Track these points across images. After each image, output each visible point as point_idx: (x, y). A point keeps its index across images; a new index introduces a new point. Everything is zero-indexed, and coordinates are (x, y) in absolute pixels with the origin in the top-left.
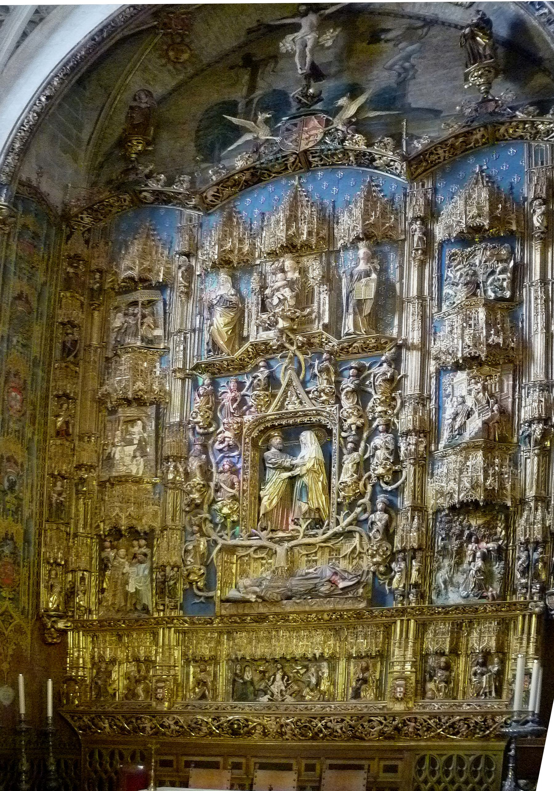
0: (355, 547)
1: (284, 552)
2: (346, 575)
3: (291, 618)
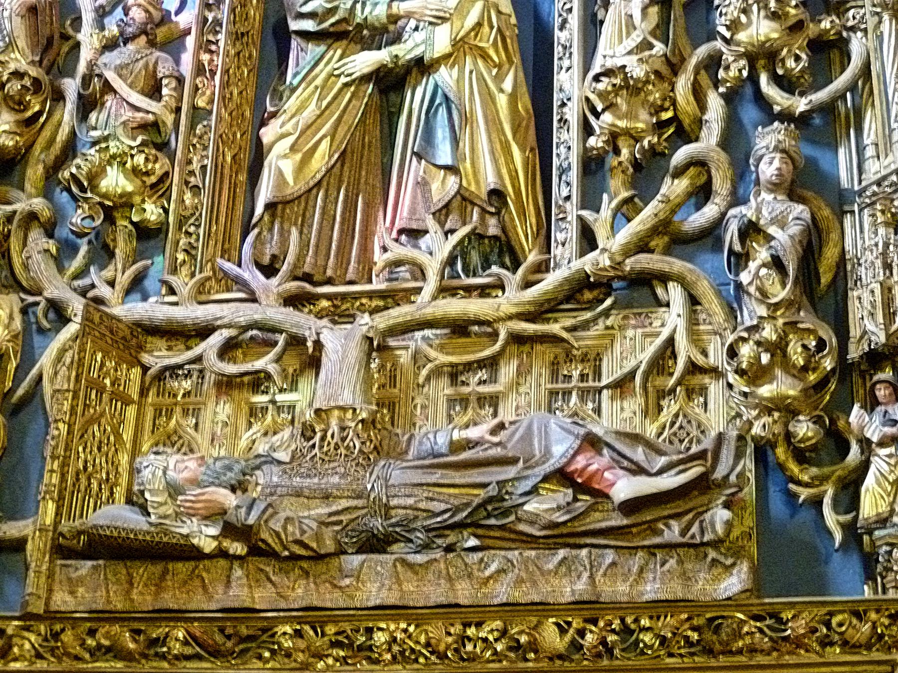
0: (670, 342)
1: (355, 352)
2: (639, 454)
3: (380, 638)
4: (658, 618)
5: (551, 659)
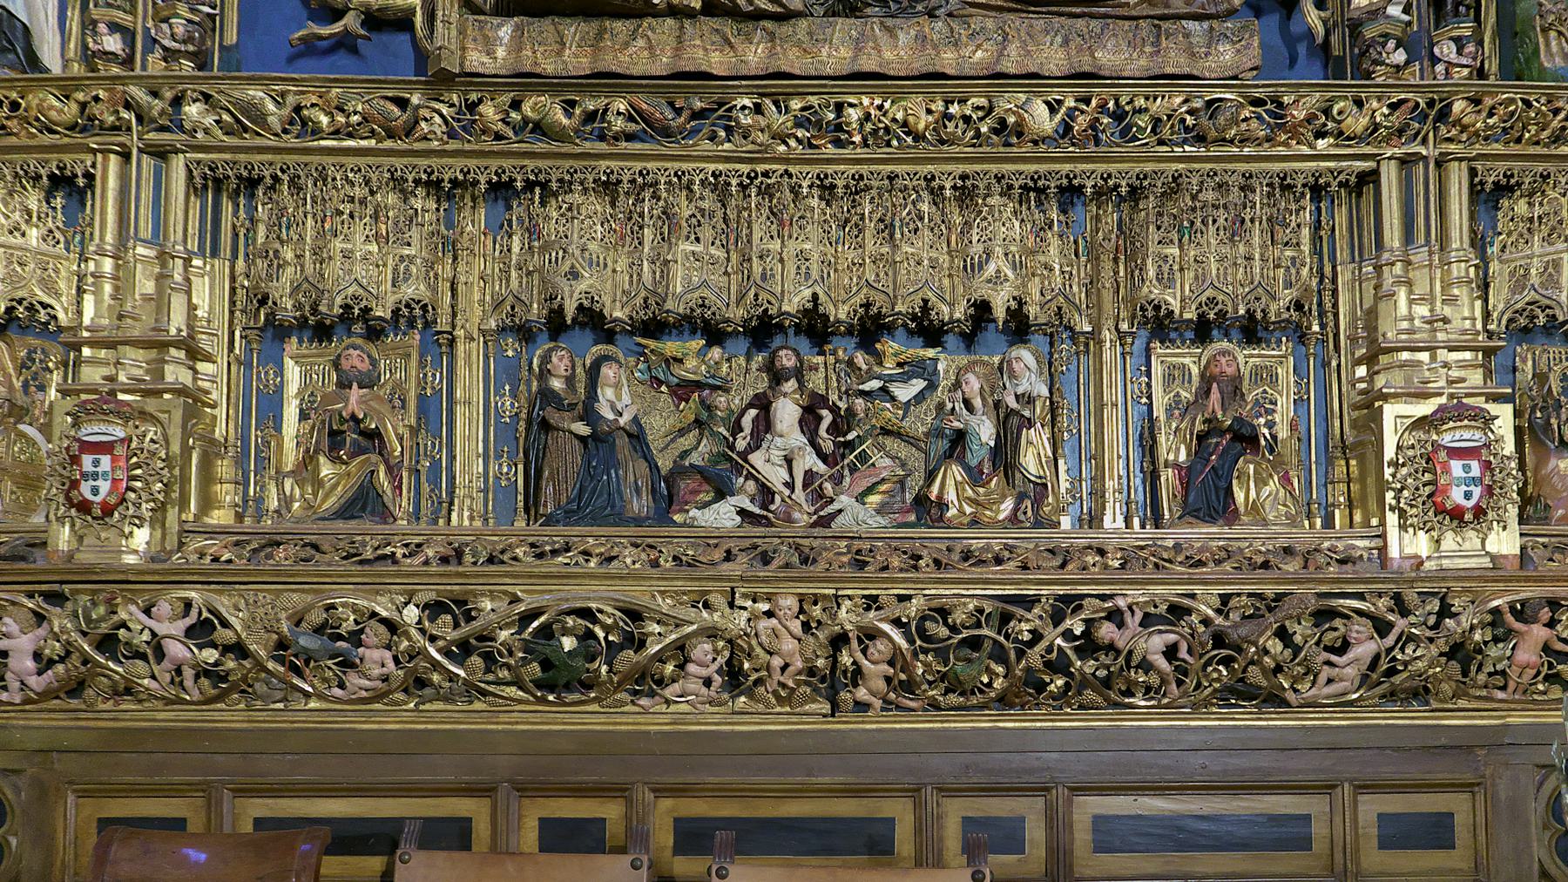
3: (854, 115)
4: (1155, 99)
5: (1035, 143)
